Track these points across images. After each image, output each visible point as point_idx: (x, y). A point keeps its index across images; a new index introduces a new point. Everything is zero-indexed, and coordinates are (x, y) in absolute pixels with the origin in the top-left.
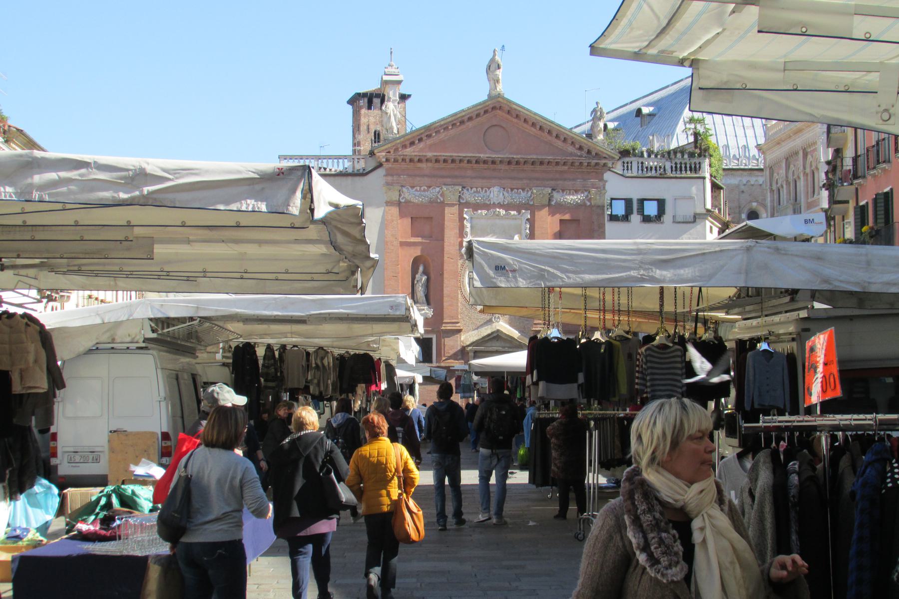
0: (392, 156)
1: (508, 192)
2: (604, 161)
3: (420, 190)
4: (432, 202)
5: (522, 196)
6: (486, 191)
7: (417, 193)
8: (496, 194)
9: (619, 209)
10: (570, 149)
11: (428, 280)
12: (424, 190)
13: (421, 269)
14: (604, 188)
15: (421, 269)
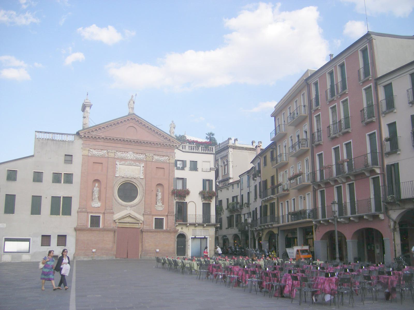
0: (87, 136)
1: (135, 154)
2: (175, 145)
3: (98, 151)
4: (102, 157)
5: (142, 157)
6: (126, 154)
7: (96, 152)
8: (130, 155)
9: (179, 164)
10: (162, 138)
11: (100, 191)
12: (100, 151)
13: (97, 185)
14: (175, 155)
15: (97, 185)
